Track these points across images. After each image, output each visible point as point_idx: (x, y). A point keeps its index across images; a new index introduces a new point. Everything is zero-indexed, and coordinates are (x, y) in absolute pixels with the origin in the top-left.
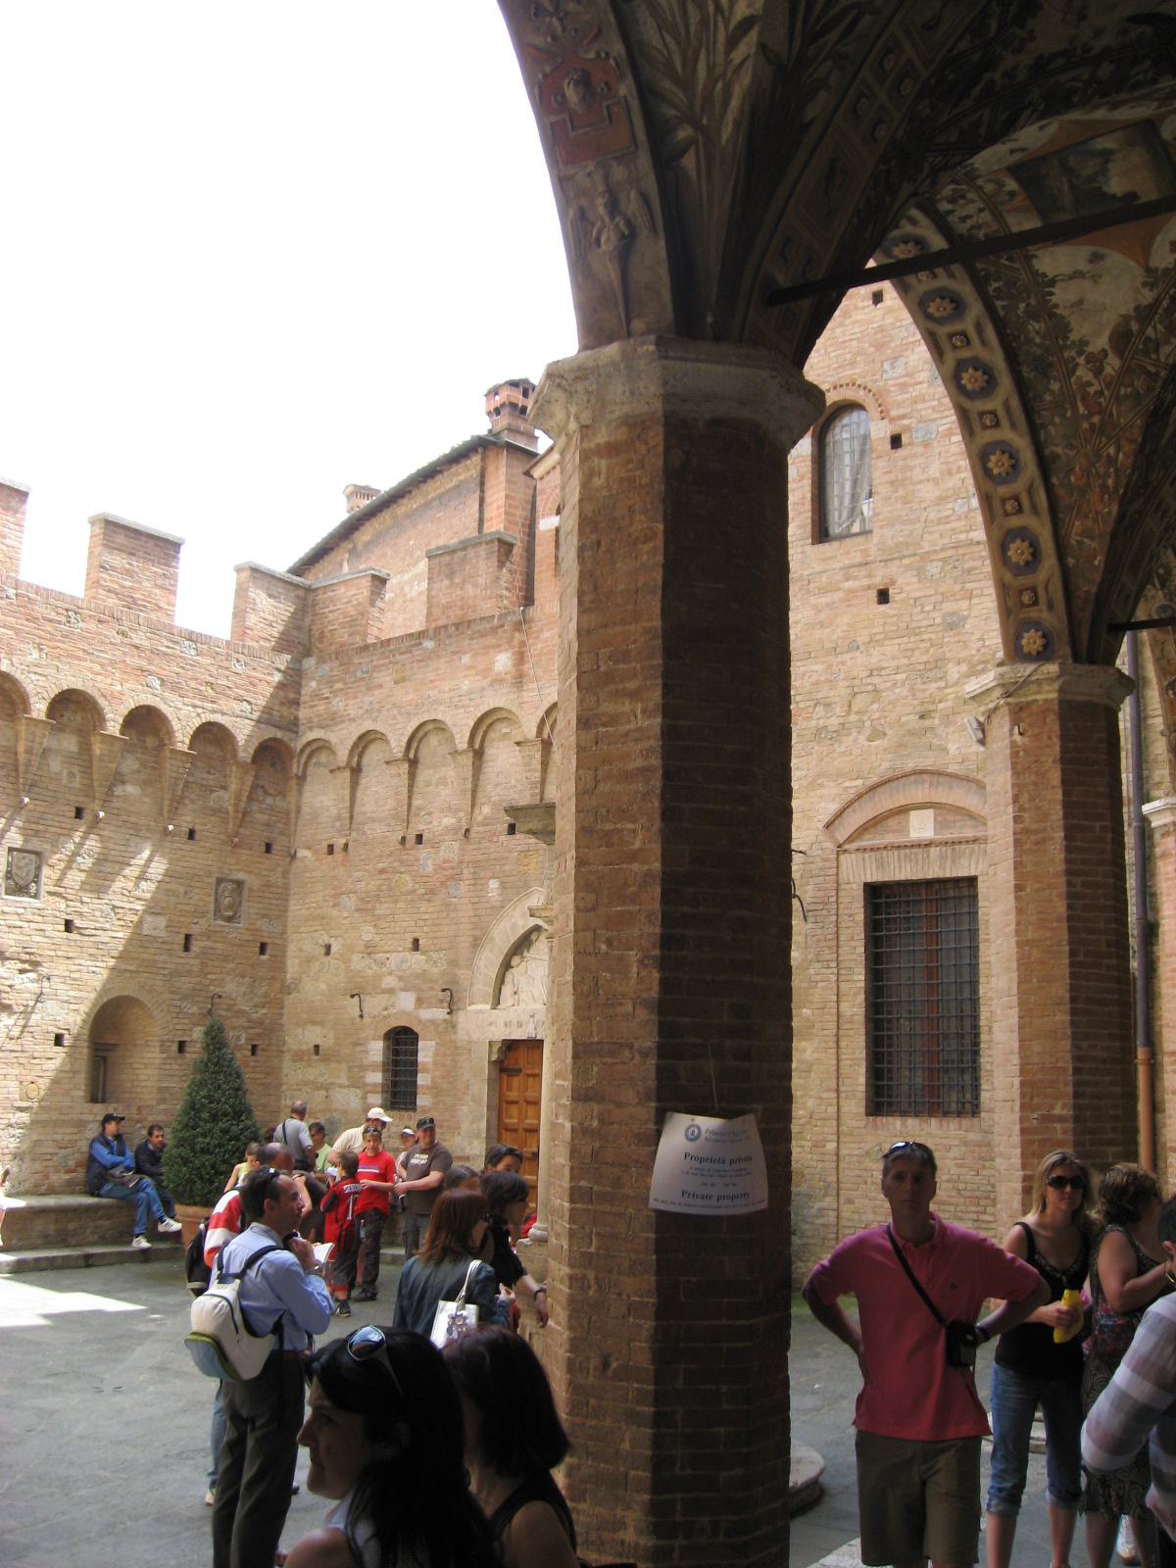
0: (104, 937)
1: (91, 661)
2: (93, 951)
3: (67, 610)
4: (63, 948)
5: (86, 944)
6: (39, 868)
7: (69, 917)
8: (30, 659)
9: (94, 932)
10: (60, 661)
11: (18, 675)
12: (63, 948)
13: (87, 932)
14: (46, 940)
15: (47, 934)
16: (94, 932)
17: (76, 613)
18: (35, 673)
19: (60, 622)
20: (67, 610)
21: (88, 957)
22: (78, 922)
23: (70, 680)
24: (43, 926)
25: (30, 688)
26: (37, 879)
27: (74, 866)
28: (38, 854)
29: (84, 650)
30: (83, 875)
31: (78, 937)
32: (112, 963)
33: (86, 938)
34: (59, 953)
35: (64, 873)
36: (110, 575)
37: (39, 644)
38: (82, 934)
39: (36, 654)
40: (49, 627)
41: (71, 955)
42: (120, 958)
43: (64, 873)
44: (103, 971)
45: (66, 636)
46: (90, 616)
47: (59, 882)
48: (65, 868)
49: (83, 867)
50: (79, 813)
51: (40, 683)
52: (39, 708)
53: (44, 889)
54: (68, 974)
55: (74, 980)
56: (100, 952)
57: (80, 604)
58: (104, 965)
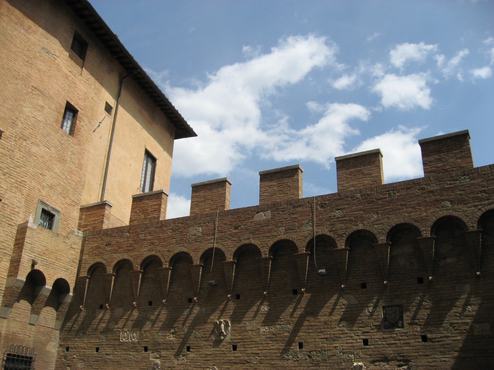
0: (448, 341)
1: (406, 208)
2: (443, 349)
3: (388, 191)
4: (422, 350)
5: (437, 347)
6: (401, 313)
7: (423, 334)
8: (372, 219)
9: (440, 339)
10: (389, 214)
11: (368, 228)
12: (422, 350)
13: (435, 340)
14: (411, 348)
15: (411, 345)
16: (440, 339)
17: (393, 191)
18: (376, 224)
19: (386, 198)
20: (388, 191)
21: (439, 353)
22: (429, 336)
23: (395, 220)
24: (408, 341)
25: (375, 232)
26: (401, 318)
27: (422, 307)
28: (400, 306)
29: (401, 205)
30: (428, 311)
31: (430, 343)
32: (456, 354)
33: (437, 343)
34: (420, 353)
35: (416, 312)
36: (429, 165)
37: (376, 211)
38: (433, 342)
39: (375, 216)
40: (380, 202)
41: (427, 353)
42: (462, 350)
43: (416, 312)
44: (450, 360)
45: (390, 202)
46: (401, 189)
47: (414, 318)
48: (416, 310)
49: (427, 307)
50: (420, 280)
51: (380, 228)
52: (382, 239)
53: (405, 324)
54: (427, 364)
55: (432, 366)
56: (447, 350)
57: (395, 186)
58: (451, 356)
